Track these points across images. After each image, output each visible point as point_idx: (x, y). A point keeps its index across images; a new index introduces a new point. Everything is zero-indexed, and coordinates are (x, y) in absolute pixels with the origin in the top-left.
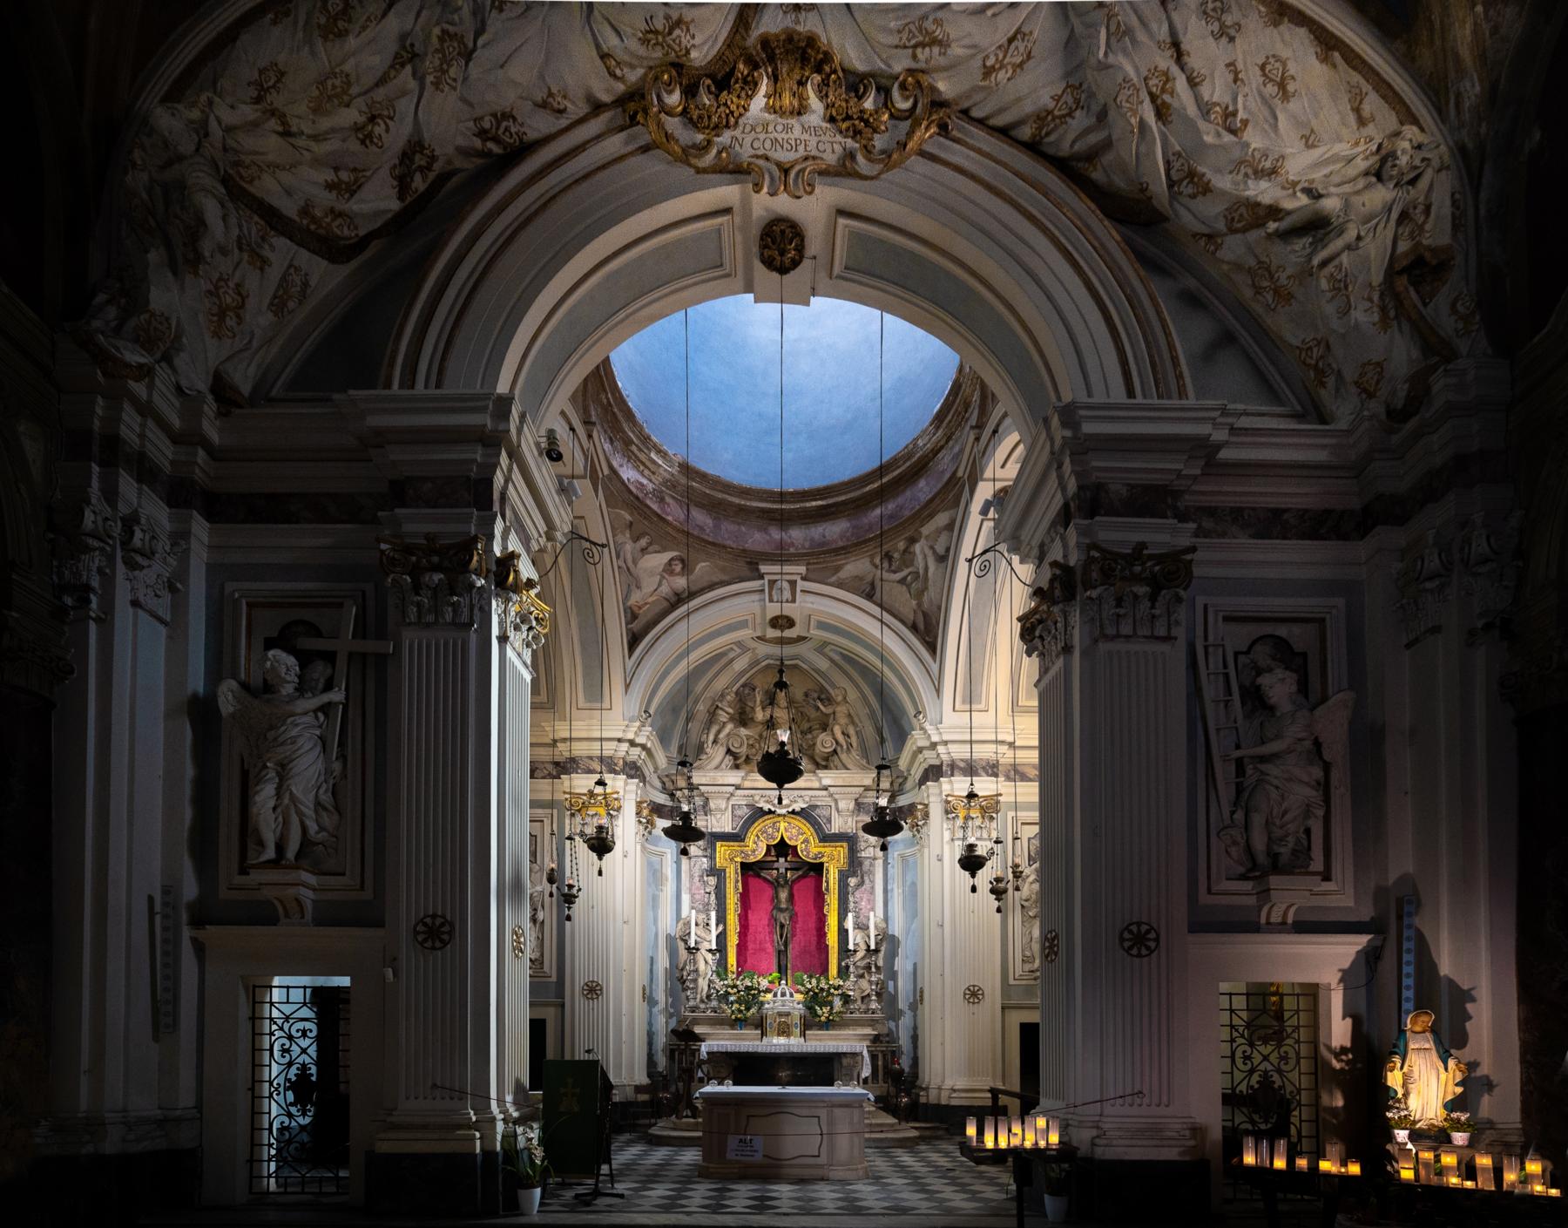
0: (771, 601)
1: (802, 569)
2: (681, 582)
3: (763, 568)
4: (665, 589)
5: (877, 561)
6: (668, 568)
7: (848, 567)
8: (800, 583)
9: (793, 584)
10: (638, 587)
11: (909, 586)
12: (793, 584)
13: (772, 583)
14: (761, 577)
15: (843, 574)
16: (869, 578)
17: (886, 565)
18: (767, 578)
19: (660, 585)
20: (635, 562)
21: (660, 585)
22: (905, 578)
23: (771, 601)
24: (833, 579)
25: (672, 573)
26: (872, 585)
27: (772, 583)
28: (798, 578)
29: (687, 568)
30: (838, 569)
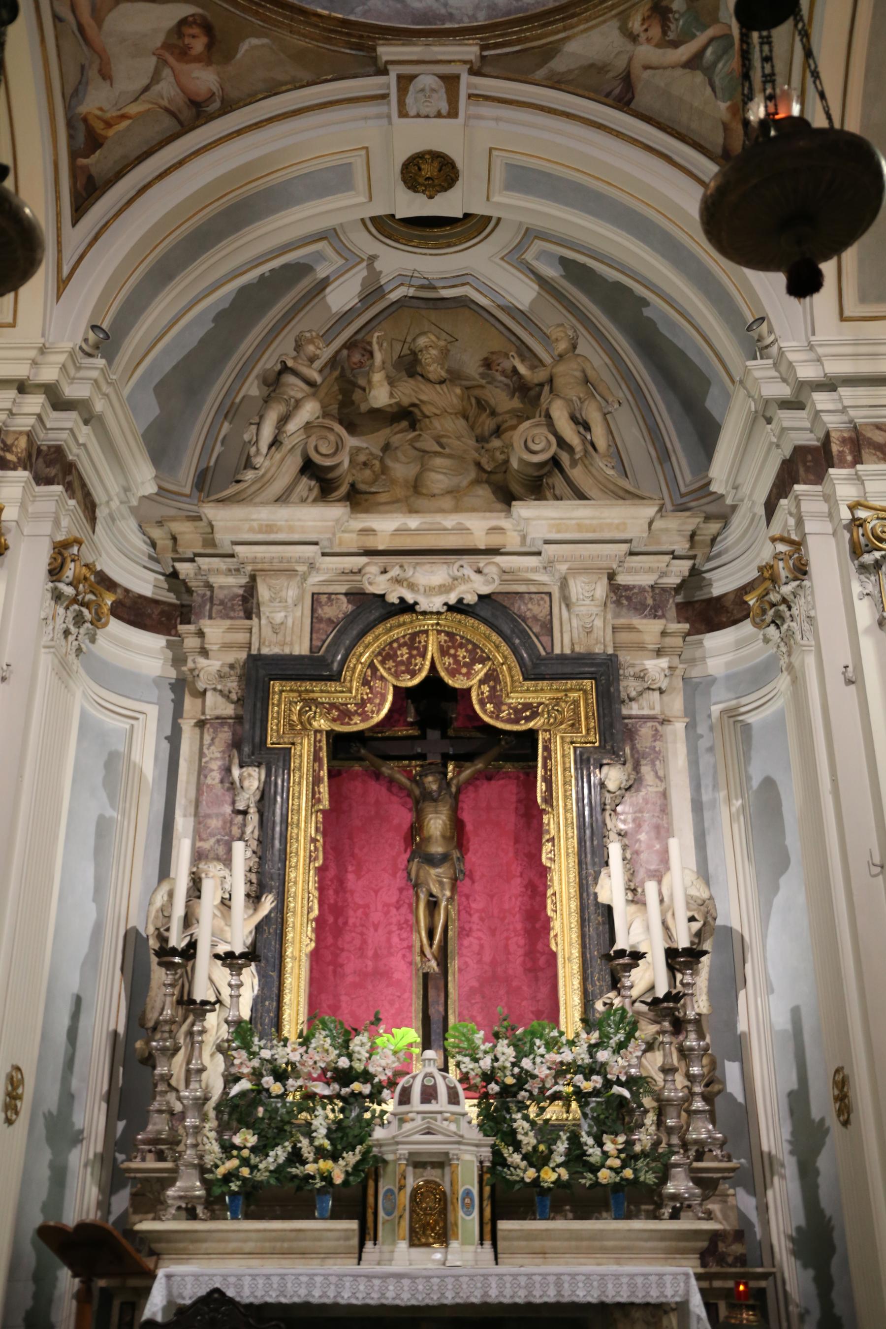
0: (403, 114)
1: (470, 51)
2: (205, 79)
3: (386, 52)
4: (167, 89)
5: (636, 24)
6: (175, 46)
7: (572, 47)
8: (465, 79)
9: (451, 82)
10: (106, 75)
11: (709, 72)
12: (451, 82)
13: (405, 81)
14: (383, 71)
15: (559, 65)
16: (621, 64)
17: (656, 31)
18: (394, 71)
19: (156, 78)
20: (98, 17)
21: (156, 78)
22: (699, 55)
23: (403, 114)
24: (540, 74)
25: (183, 54)
26: (627, 79)
27: (405, 81)
28: (463, 72)
29: (218, 48)
30: (550, 52)
